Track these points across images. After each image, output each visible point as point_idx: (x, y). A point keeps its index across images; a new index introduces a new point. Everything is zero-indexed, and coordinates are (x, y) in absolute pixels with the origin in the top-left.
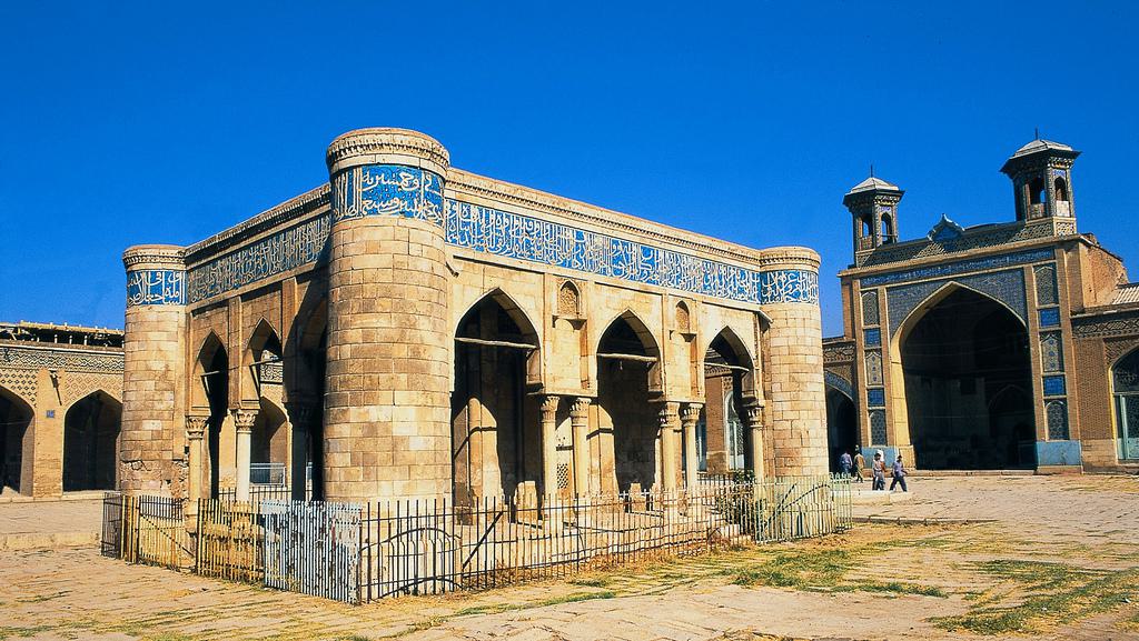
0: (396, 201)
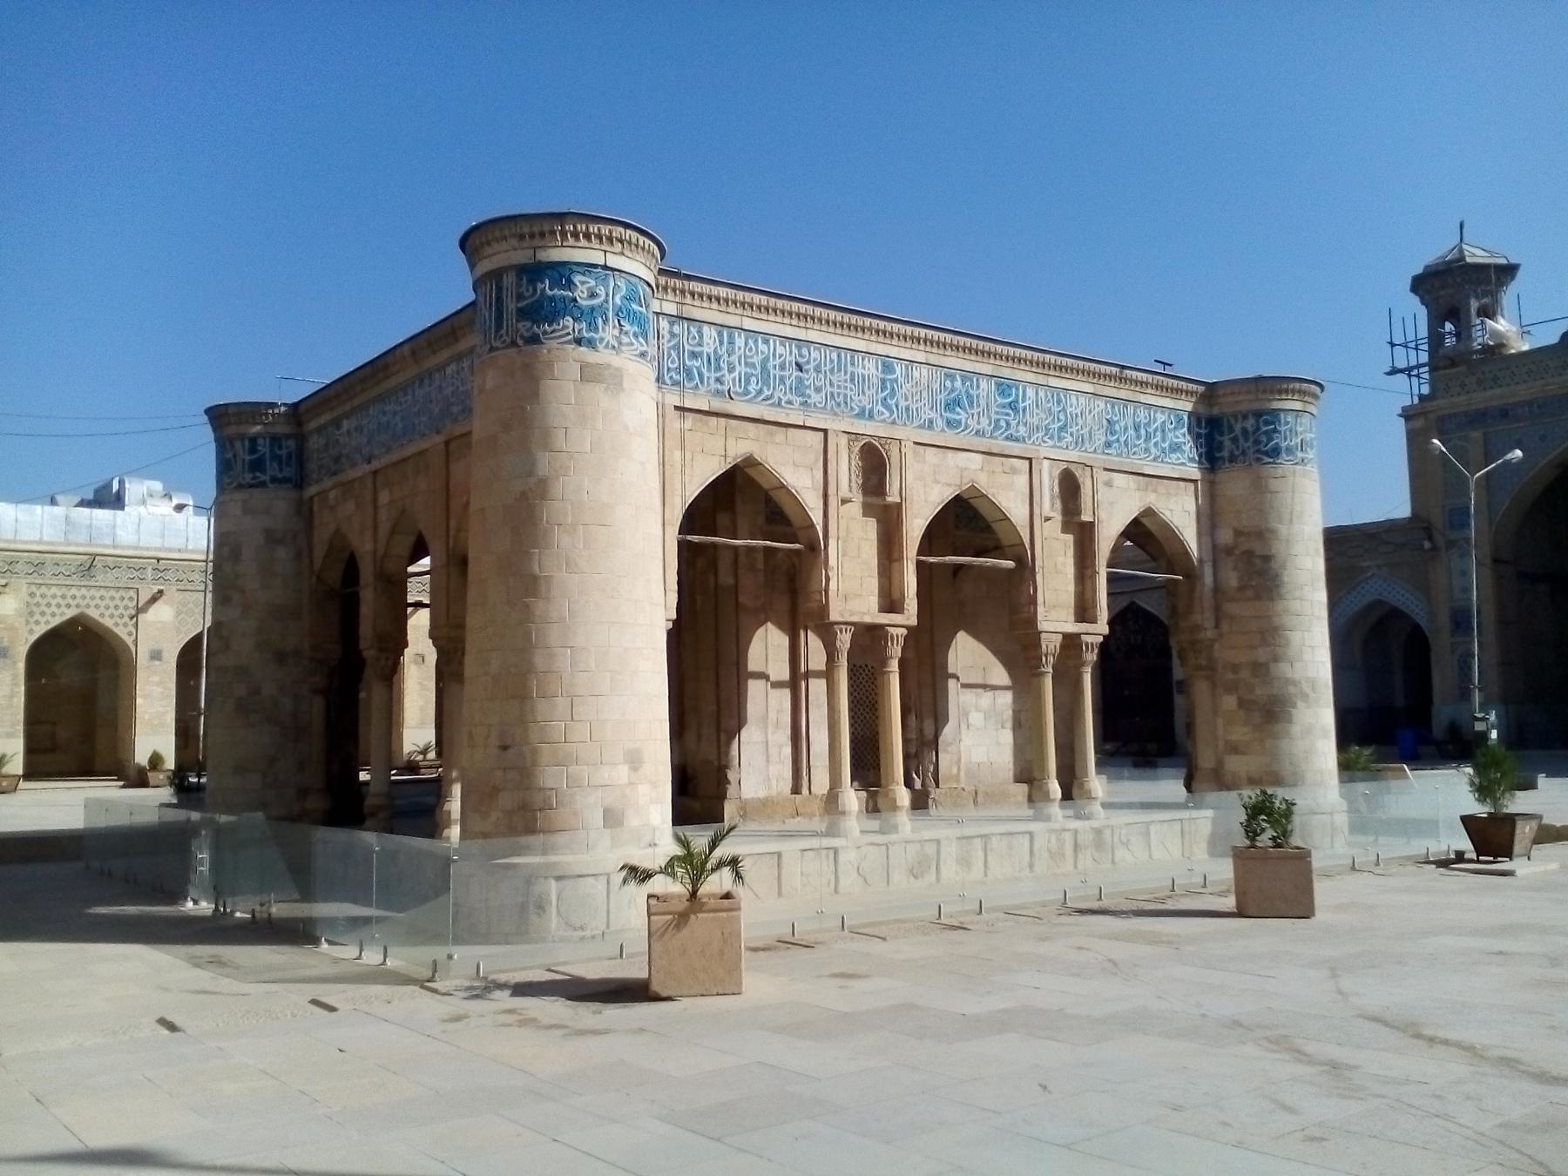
0: (569, 321)
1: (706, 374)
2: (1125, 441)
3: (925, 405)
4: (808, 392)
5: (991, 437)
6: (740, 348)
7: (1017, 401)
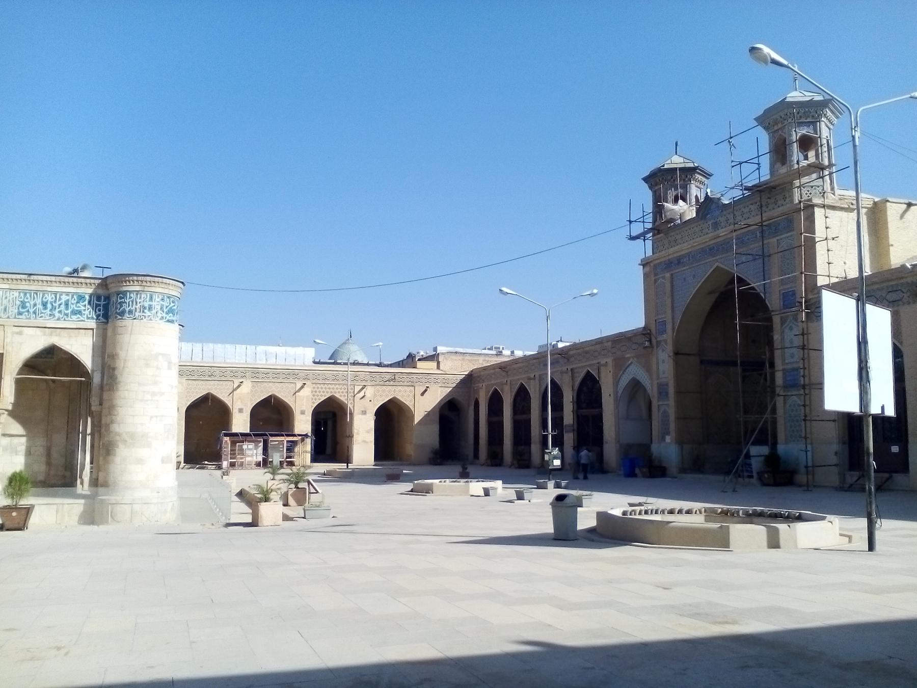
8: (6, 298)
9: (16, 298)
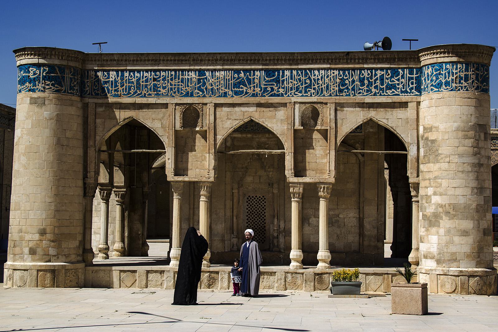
0: (27, 84)
1: (111, 89)
2: (352, 89)
3: (222, 87)
4: (159, 89)
5: (262, 96)
6: (126, 77)
7: (278, 77)
8: (328, 77)
9: (336, 76)
